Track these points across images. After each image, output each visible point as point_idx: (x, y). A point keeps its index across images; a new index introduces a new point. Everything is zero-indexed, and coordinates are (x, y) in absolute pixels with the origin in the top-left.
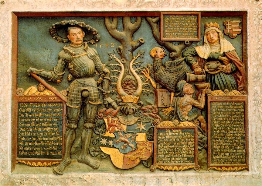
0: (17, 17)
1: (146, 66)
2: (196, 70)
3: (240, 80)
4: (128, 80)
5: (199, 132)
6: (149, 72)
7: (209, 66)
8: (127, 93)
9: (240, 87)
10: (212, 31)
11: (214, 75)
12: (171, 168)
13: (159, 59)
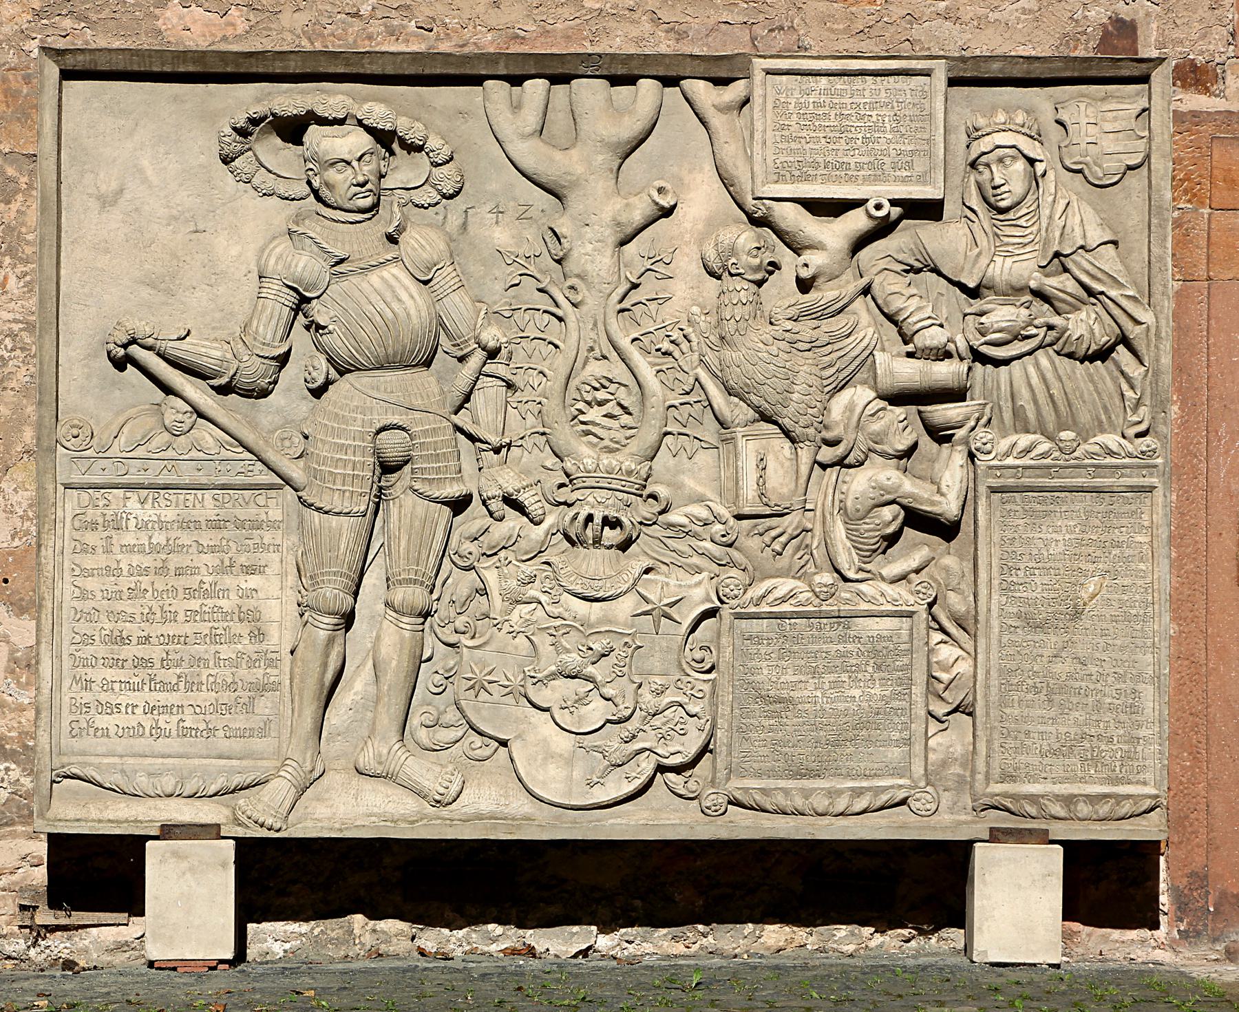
0: (61, 71)
1: (684, 317)
2: (919, 340)
3: (1132, 387)
4: (598, 385)
5: (938, 636)
6: (694, 344)
7: (983, 319)
8: (594, 445)
9: (1135, 419)
10: (1000, 152)
11: (1006, 362)
12: (799, 802)
13: (746, 285)
